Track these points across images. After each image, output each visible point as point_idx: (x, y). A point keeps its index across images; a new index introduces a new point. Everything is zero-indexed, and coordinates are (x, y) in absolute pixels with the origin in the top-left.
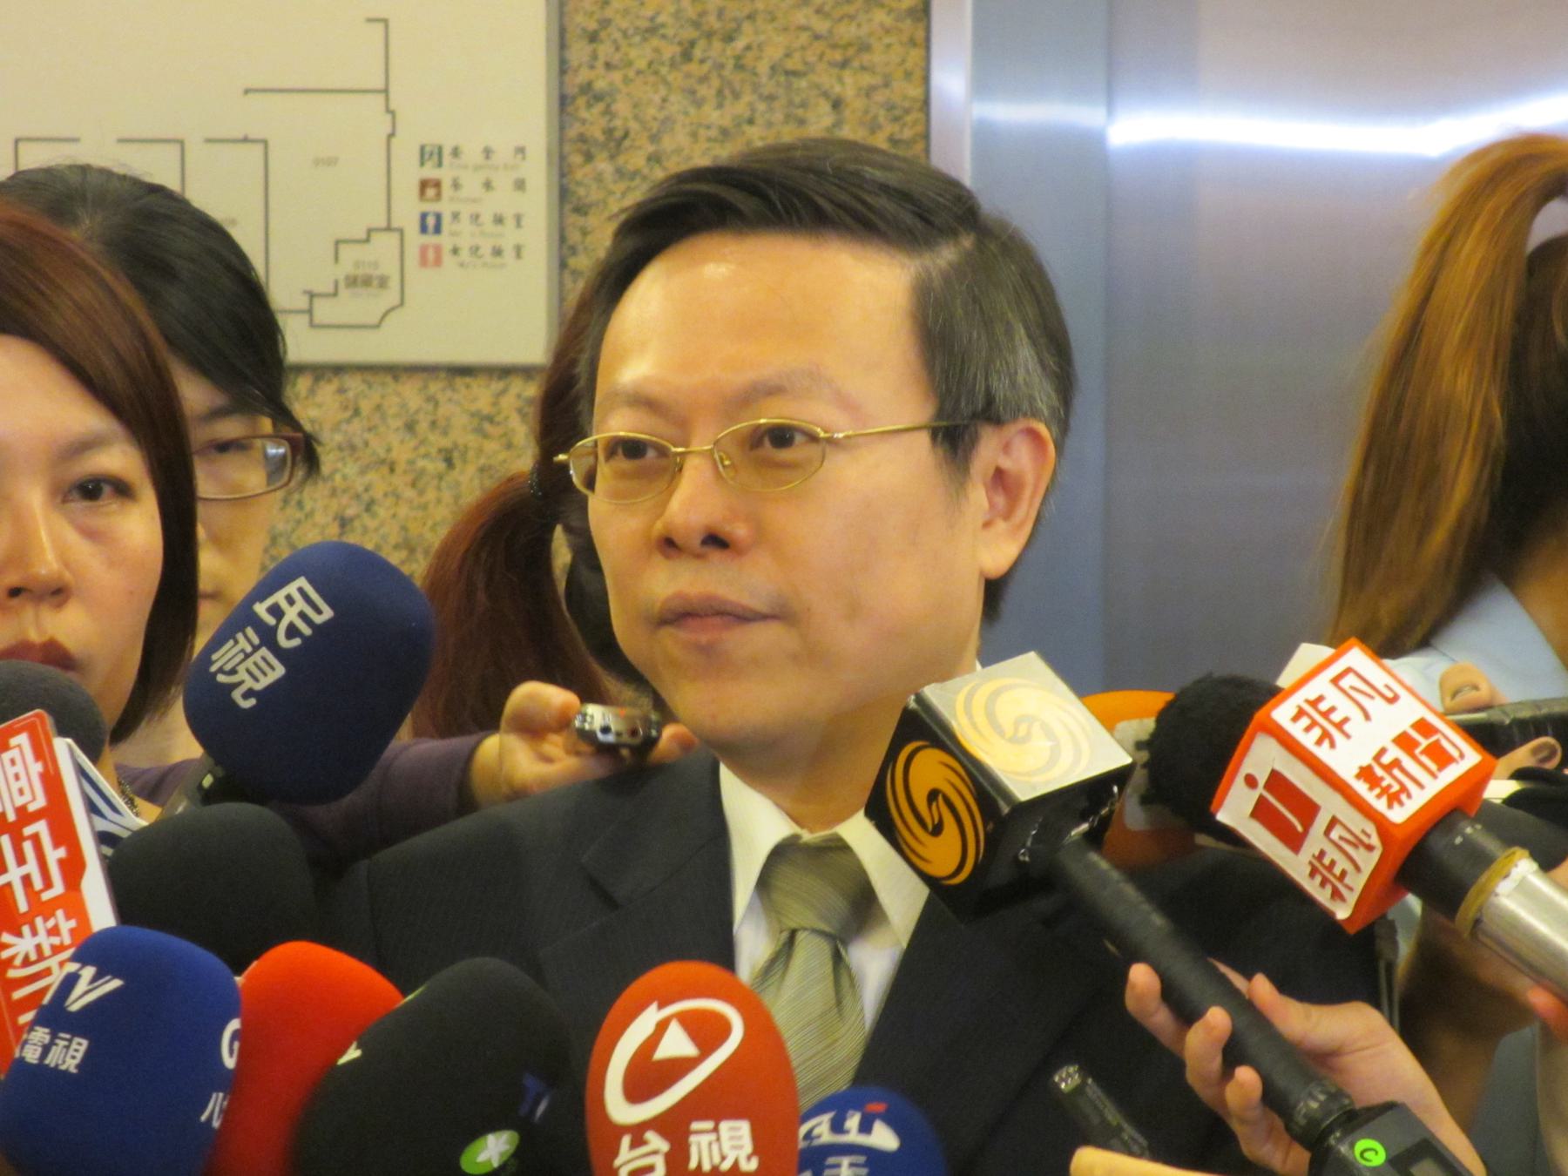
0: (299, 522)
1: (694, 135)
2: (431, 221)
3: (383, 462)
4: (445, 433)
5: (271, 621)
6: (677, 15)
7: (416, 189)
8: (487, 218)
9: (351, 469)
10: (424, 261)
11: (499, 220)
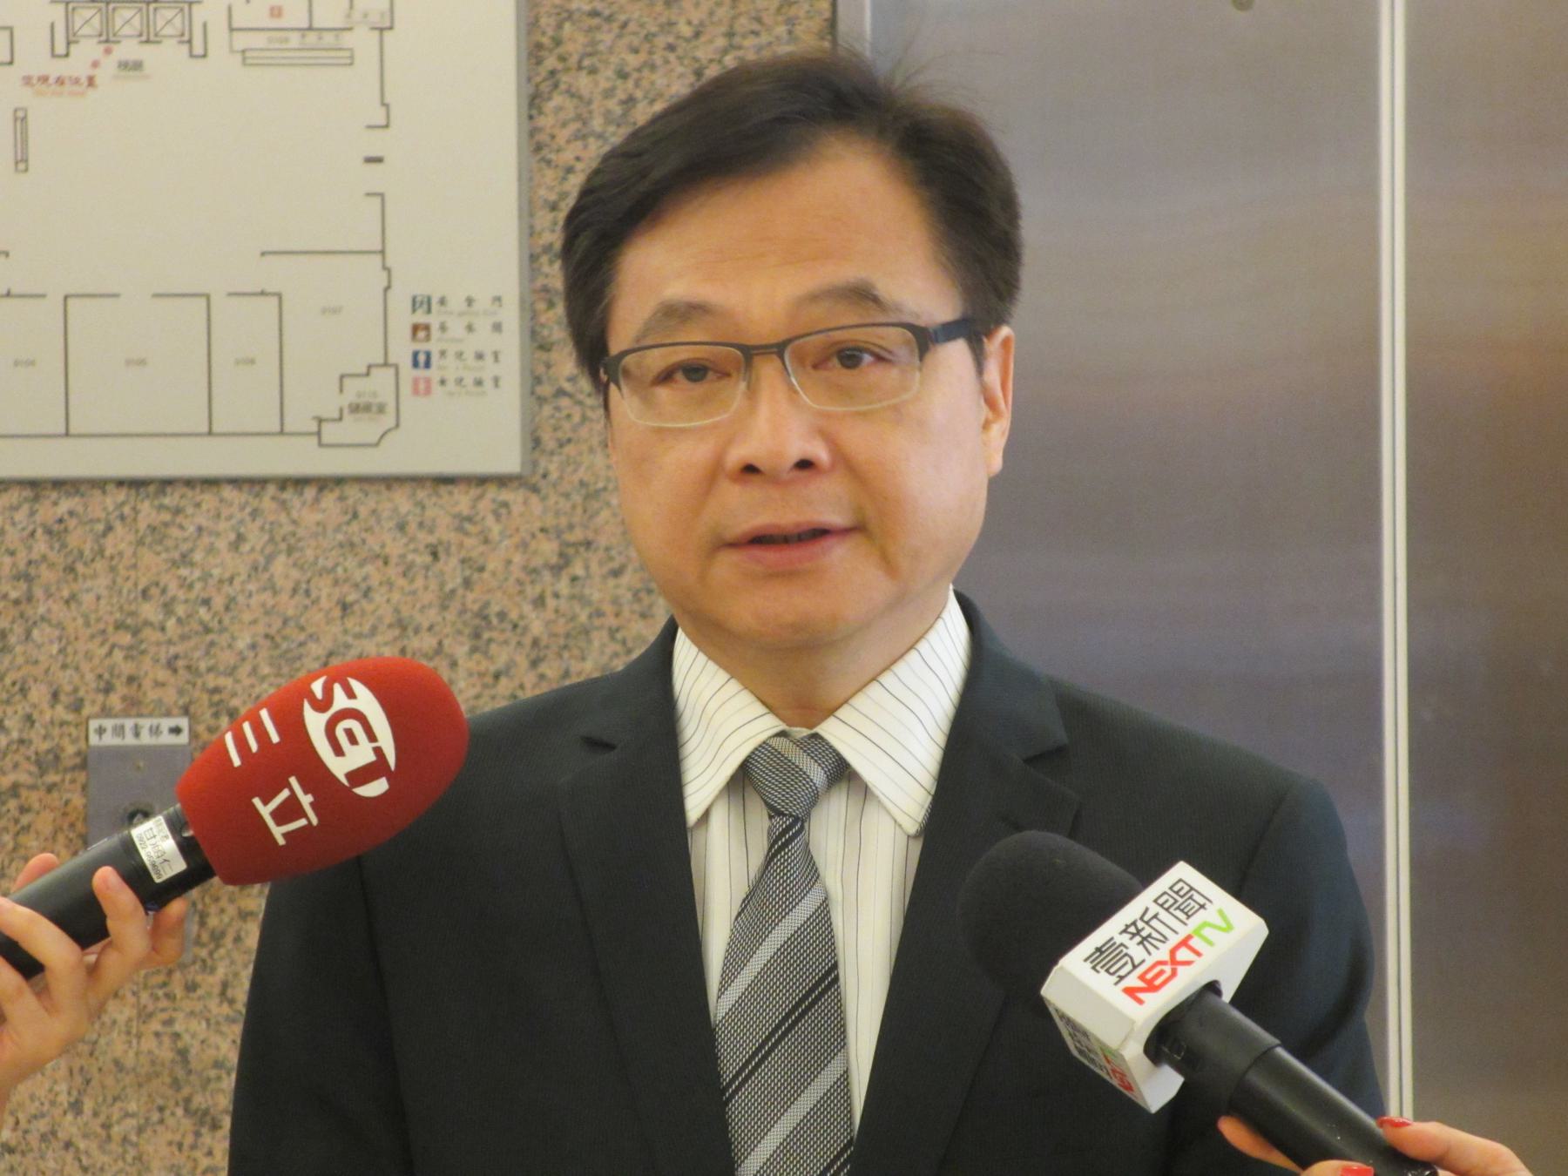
0: (306, 607)
2: (422, 358)
3: (378, 556)
4: (431, 532)
7: (408, 331)
8: (469, 356)
9: (351, 563)
10: (416, 391)
11: (480, 356)
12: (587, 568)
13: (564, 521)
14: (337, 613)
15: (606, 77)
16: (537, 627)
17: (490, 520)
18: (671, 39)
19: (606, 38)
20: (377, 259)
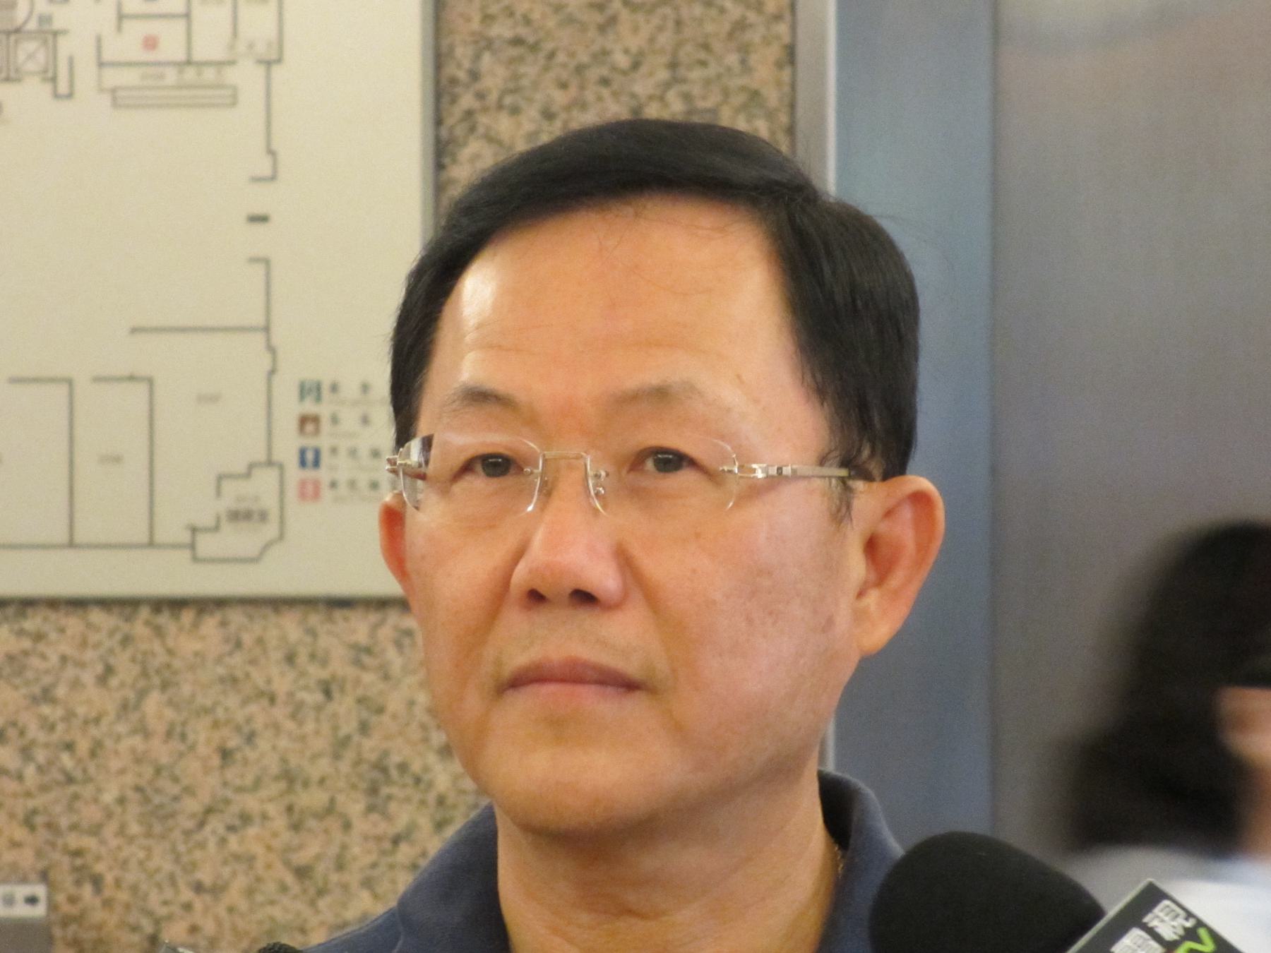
2: (310, 456)
19: (530, 70)
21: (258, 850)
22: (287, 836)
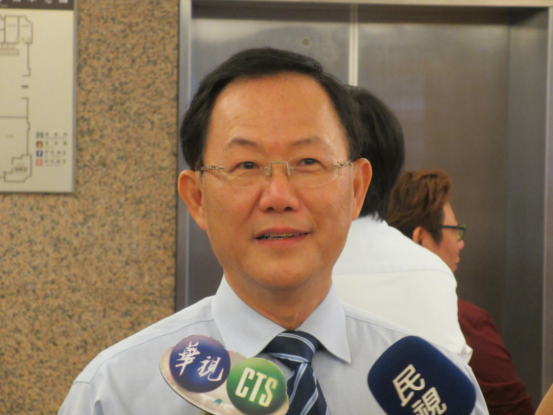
1: (113, 131)
2: (39, 153)
5: (411, 394)
6: (108, 98)
8: (56, 152)
9: (14, 221)
11: (59, 153)
12: (93, 223)
13: (85, 208)
14: (9, 237)
15: (103, 60)
16: (76, 243)
17: (61, 208)
18: (124, 49)
19: (103, 48)
20: (25, 121)
21: (21, 261)
22: (30, 258)
